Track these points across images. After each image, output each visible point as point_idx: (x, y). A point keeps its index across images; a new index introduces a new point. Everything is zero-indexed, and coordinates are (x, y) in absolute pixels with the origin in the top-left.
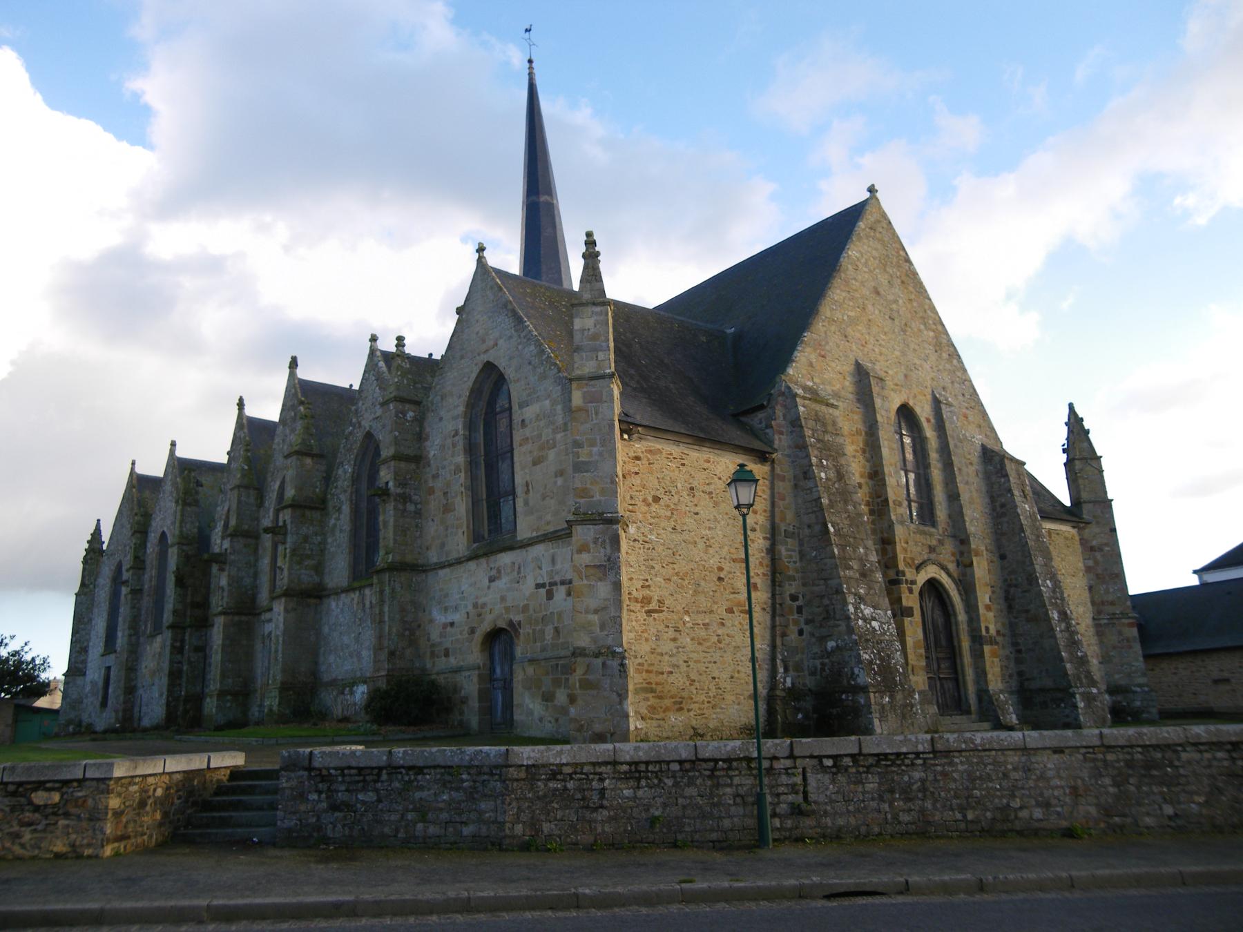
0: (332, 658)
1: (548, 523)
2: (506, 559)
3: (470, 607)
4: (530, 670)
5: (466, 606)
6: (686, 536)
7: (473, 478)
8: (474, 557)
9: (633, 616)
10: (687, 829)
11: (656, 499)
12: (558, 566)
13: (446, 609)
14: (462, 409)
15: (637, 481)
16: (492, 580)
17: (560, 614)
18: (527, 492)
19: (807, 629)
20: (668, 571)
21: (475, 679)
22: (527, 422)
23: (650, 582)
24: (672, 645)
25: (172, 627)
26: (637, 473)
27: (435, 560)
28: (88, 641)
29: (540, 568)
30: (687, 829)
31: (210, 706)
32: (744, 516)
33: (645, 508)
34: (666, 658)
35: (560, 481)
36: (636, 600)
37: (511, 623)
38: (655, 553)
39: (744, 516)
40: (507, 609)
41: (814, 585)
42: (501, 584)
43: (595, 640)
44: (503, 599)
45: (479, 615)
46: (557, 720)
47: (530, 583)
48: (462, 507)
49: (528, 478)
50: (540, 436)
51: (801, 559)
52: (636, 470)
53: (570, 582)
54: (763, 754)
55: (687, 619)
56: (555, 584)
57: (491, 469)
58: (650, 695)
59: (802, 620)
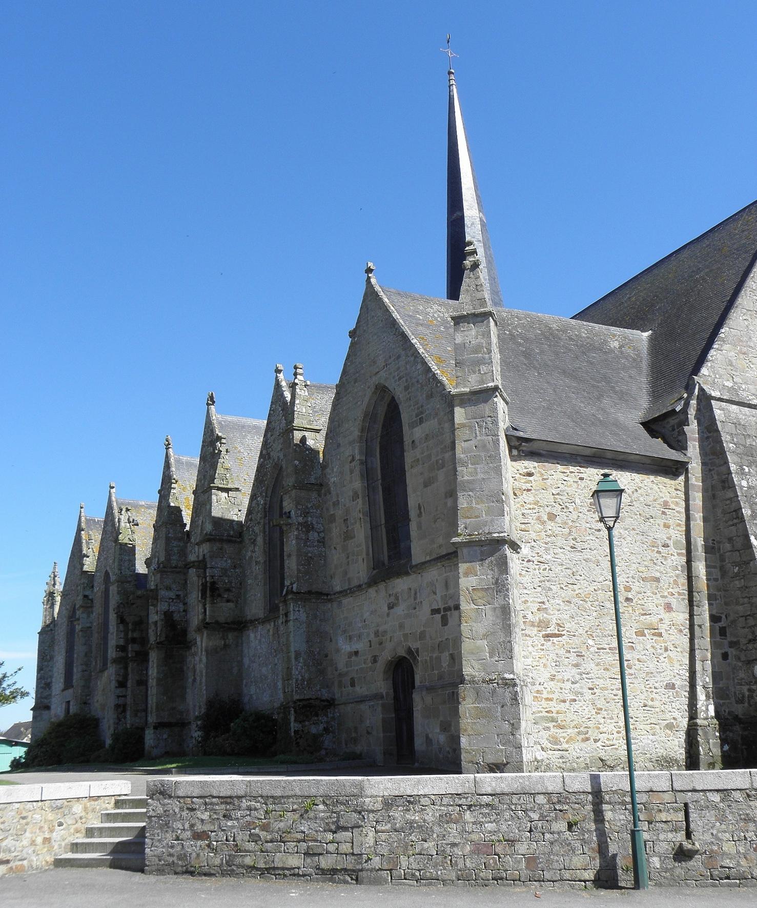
0: (253, 690)
1: (440, 546)
2: (401, 584)
3: (372, 635)
4: (428, 699)
5: (368, 634)
6: (587, 554)
7: (371, 503)
8: (373, 582)
9: (529, 642)
10: (556, 865)
11: (552, 517)
14: (357, 433)
15: (529, 498)
16: (391, 607)
18: (420, 515)
19: (732, 652)
20: (568, 593)
21: (379, 709)
22: (417, 442)
23: (547, 605)
24: (575, 670)
25: (115, 661)
26: (529, 490)
28: (51, 677)
29: (435, 593)
30: (556, 865)
31: (150, 737)
32: (610, 529)
33: (538, 527)
34: (568, 685)
36: (532, 624)
37: (409, 651)
38: (551, 574)
39: (610, 529)
40: (405, 636)
41: (737, 603)
42: (400, 610)
43: (485, 668)
44: (401, 626)
45: (381, 644)
47: (424, 612)
48: (361, 534)
50: (430, 456)
51: (723, 576)
52: (528, 486)
54: (637, 786)
55: (591, 642)
57: (388, 492)
58: (551, 725)
59: (726, 642)
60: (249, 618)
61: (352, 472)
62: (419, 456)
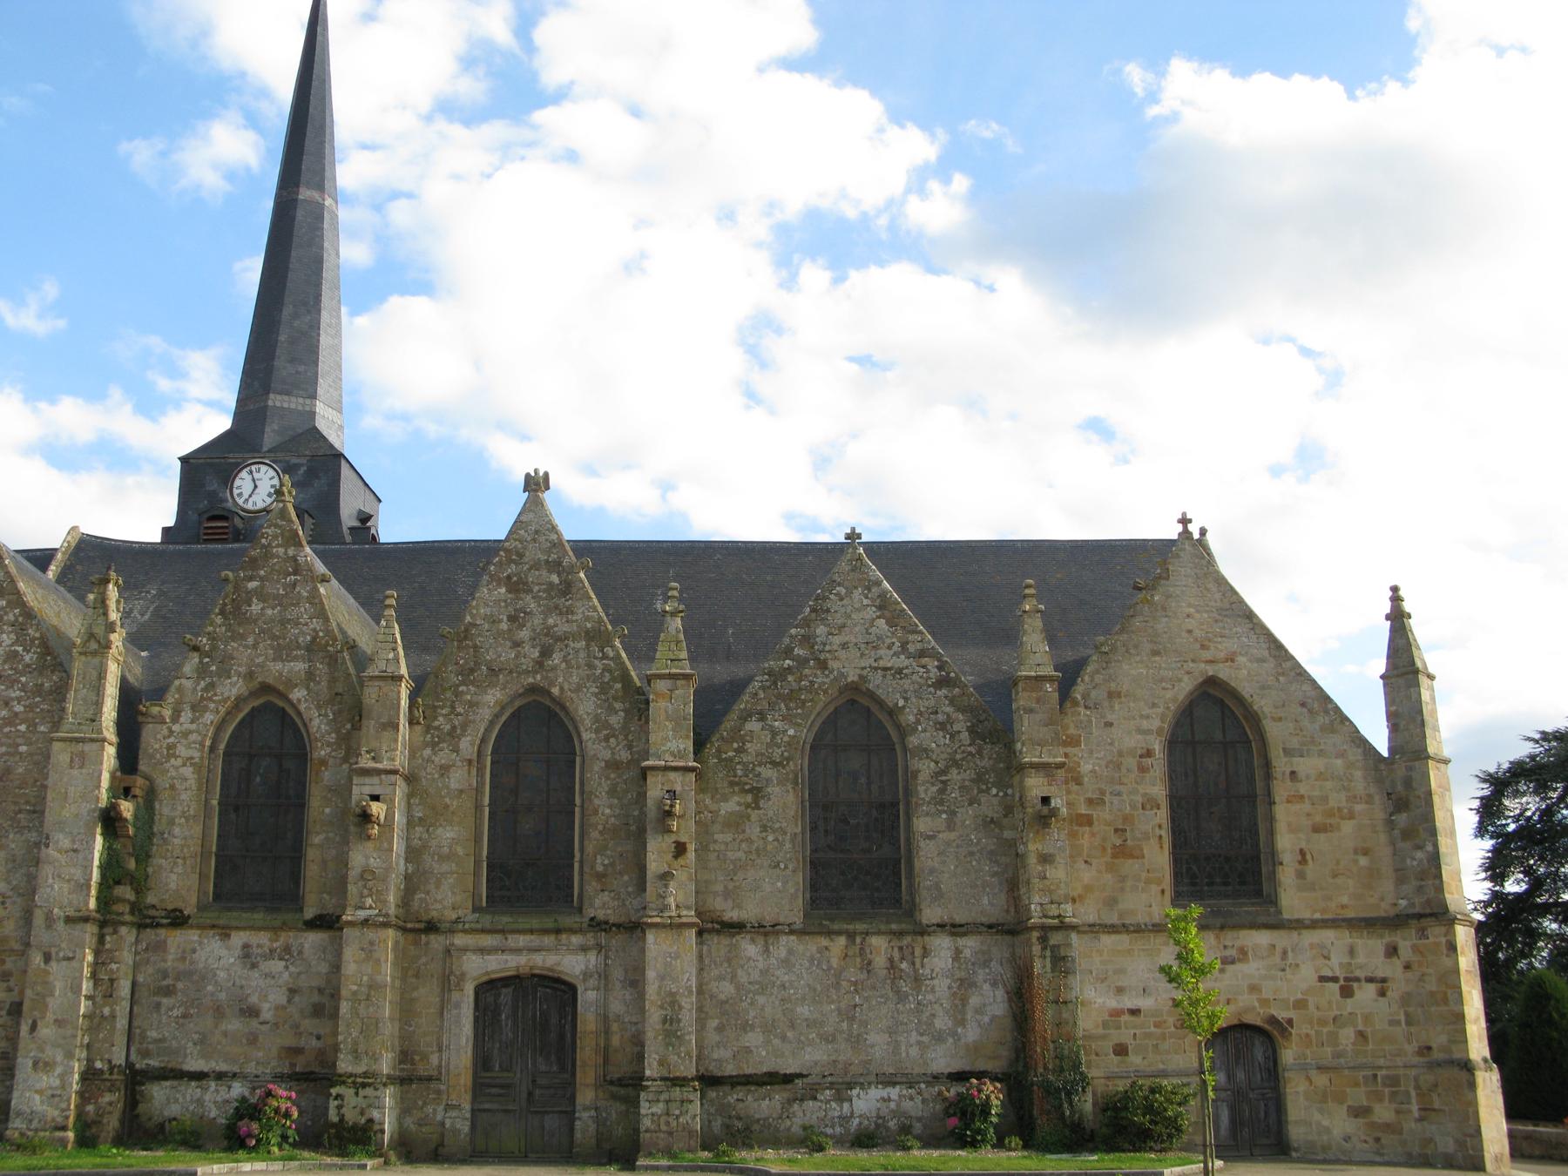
1: (1343, 907)
12: (1361, 959)
13: (1120, 990)
17: (1367, 1018)
18: (1303, 861)
27: (1091, 919)
29: (1327, 958)
40: (1265, 1002)
46: (1378, 1140)
47: (1307, 974)
53: (1384, 980)
56: (1357, 980)
60: (732, 915)
62: (1302, 792)
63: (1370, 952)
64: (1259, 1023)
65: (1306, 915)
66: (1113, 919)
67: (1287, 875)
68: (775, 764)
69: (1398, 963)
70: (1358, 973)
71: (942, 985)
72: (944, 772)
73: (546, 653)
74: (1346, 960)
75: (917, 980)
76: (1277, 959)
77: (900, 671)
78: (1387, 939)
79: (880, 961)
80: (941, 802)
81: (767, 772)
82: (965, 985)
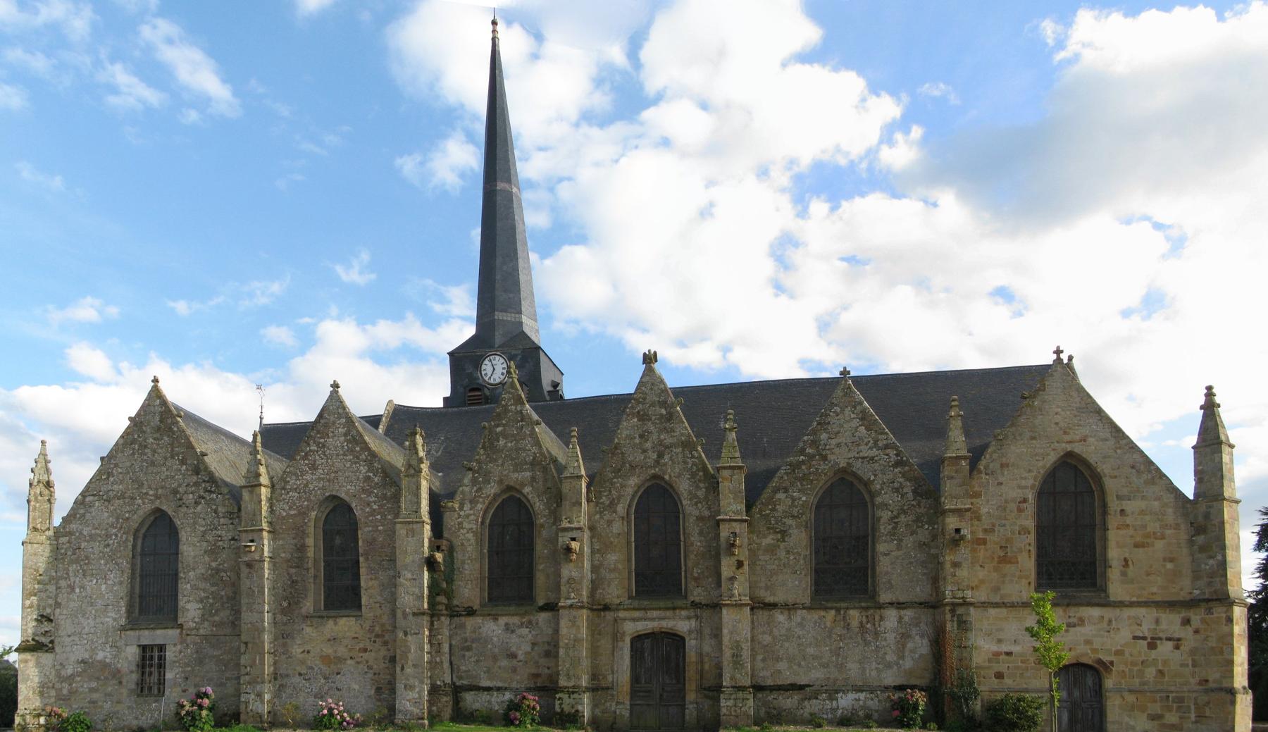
4: (1131, 698)
12: (1163, 626)
13: (1000, 641)
17: (1165, 662)
35: (1169, 566)
37: (1100, 662)
40: (1095, 651)
47: (1125, 635)
49: (1127, 555)
50: (1145, 527)
53: (1179, 640)
56: (1160, 639)
61: (1020, 510)
63: (1171, 623)
64: (1090, 663)
65: (1127, 598)
66: (997, 599)
67: (1114, 574)
68: (793, 517)
69: (1190, 630)
70: (1161, 635)
71: (891, 637)
72: (896, 517)
73: (661, 455)
74: (1153, 627)
75: (877, 634)
76: (1105, 625)
77: (872, 459)
78: (1183, 615)
79: (855, 624)
80: (894, 534)
81: (789, 521)
82: (905, 636)
